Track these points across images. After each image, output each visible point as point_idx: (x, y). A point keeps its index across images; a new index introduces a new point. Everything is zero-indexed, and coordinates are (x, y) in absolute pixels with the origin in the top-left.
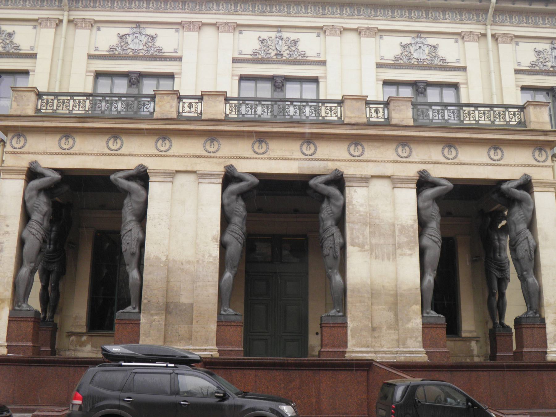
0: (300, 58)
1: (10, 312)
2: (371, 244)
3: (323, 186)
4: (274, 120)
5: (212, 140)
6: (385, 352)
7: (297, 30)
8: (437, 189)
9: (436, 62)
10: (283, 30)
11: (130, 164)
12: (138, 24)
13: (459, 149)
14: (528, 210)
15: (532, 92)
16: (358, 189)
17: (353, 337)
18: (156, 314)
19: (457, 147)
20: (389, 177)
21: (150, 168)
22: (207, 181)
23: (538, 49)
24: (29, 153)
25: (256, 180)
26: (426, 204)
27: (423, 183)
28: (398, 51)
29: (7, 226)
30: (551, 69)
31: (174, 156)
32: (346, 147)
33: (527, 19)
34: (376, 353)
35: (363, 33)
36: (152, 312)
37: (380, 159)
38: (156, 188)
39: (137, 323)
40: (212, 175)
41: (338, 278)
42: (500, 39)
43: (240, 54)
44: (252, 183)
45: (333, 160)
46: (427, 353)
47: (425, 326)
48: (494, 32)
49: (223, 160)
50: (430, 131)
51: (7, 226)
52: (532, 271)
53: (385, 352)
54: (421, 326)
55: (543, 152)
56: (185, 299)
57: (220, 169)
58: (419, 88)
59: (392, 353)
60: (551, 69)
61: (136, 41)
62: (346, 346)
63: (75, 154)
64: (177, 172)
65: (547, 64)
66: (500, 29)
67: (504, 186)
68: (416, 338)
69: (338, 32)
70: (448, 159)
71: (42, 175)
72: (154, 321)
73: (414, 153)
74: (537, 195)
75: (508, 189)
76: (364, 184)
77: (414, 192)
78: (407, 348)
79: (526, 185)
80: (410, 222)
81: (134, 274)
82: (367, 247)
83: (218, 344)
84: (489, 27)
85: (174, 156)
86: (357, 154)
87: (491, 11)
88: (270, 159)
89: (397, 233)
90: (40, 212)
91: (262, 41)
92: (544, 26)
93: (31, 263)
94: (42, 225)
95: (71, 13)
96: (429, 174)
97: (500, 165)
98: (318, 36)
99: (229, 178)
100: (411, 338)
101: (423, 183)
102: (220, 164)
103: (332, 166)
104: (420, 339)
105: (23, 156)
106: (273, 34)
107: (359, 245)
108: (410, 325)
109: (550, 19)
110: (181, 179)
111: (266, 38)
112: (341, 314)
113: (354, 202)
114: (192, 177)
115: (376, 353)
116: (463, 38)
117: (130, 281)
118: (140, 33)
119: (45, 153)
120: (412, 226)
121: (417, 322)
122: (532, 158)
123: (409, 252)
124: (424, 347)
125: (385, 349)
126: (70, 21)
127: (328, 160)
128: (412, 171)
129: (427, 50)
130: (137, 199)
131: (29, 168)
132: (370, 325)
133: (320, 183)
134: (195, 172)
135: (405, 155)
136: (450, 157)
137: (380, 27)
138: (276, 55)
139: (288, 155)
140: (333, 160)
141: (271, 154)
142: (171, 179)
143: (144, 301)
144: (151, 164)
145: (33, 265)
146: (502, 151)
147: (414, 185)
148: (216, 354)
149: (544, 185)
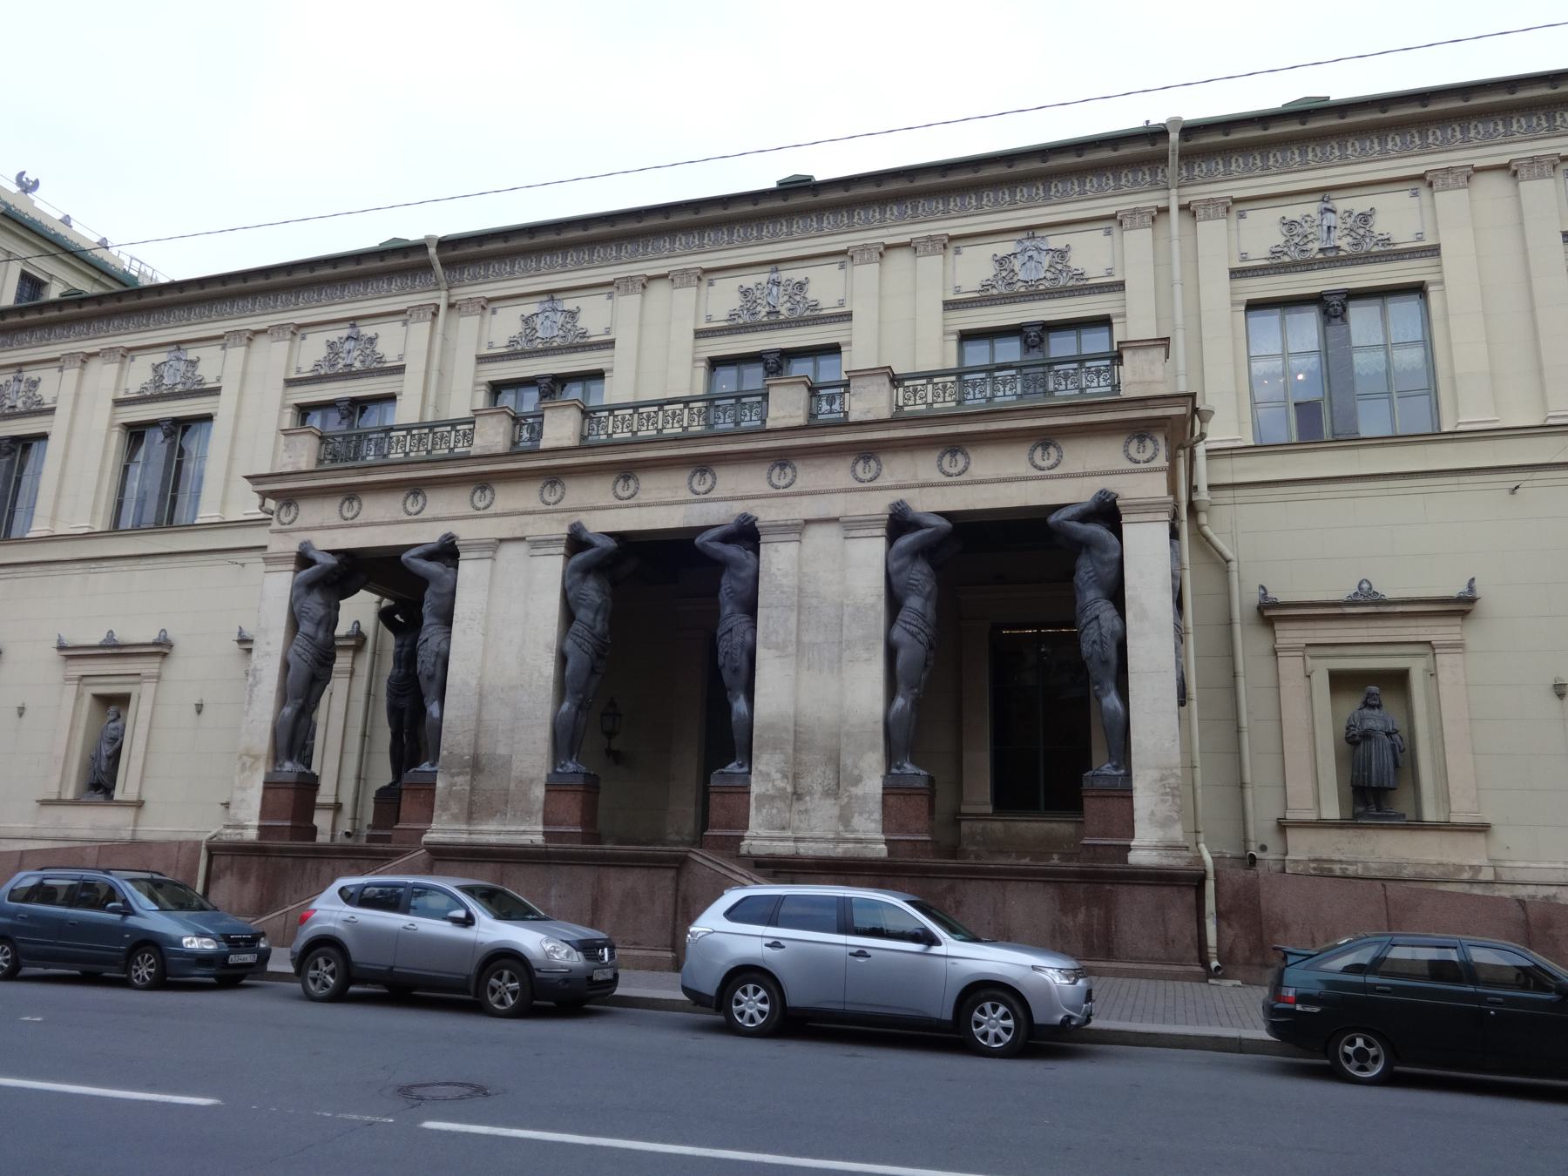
0: (808, 313)
1: (267, 774)
2: (799, 643)
3: (717, 546)
4: (710, 432)
5: (626, 478)
6: (814, 840)
7: (806, 263)
8: (919, 533)
9: (1063, 281)
10: (780, 267)
11: (430, 535)
12: (551, 293)
13: (972, 455)
14: (1103, 563)
15: (1379, 301)
16: (781, 546)
17: (758, 809)
18: (459, 774)
19: (968, 450)
20: (836, 520)
22: (542, 551)
23: (1289, 218)
24: (299, 530)
25: (611, 544)
26: (900, 562)
27: (899, 523)
28: (988, 271)
30: (1320, 256)
31: (496, 515)
32: (765, 473)
33: (1265, 158)
34: (796, 840)
35: (921, 248)
37: (829, 488)
38: (468, 569)
39: (431, 788)
40: (549, 542)
41: (740, 706)
42: (1200, 213)
43: (709, 321)
44: (604, 550)
45: (742, 498)
46: (887, 842)
47: (888, 791)
48: (1185, 201)
49: (564, 515)
50: (908, 427)
52: (1111, 685)
53: (814, 840)
54: (880, 791)
55: (1148, 443)
56: (502, 750)
57: (563, 531)
58: (1028, 337)
59: (827, 840)
60: (1320, 256)
61: (548, 323)
62: (747, 828)
63: (361, 525)
64: (501, 540)
65: (1310, 246)
66: (1197, 193)
67: (1053, 519)
68: (871, 813)
69: (876, 255)
70: (777, 488)
71: (311, 562)
73: (885, 470)
74: (1128, 531)
75: (1058, 523)
76: (793, 536)
77: (880, 545)
78: (854, 831)
79: (1107, 513)
80: (871, 600)
81: (433, 709)
82: (792, 649)
83: (546, 823)
84: (1174, 192)
85: (496, 515)
86: (783, 483)
87: (1173, 159)
88: (639, 506)
89: (846, 618)
90: (311, 619)
91: (745, 293)
92: (1305, 167)
95: (453, 291)
96: (908, 507)
97: (1052, 477)
98: (842, 267)
99: (576, 542)
100: (861, 814)
101: (899, 523)
102: (562, 521)
103: (739, 508)
104: (878, 815)
106: (763, 277)
107: (777, 647)
108: (858, 791)
109: (1318, 150)
110: (509, 552)
111: (752, 286)
112: (745, 769)
113: (773, 570)
114: (521, 548)
115: (796, 840)
116: (1121, 223)
117: (428, 720)
118: (554, 310)
120: (873, 606)
121: (873, 784)
122: (1121, 455)
123: (865, 656)
124: (883, 832)
125: (817, 833)
126: (451, 306)
127: (733, 499)
128: (878, 505)
129: (1046, 260)
130: (438, 590)
132: (790, 789)
133: (711, 540)
134: (522, 539)
135: (869, 476)
136: (954, 471)
137: (952, 233)
138: (769, 313)
139: (667, 496)
140: (742, 498)
141: (642, 497)
142: (490, 554)
143: (443, 753)
144: (465, 532)
146: (1059, 449)
147: (882, 531)
148: (539, 839)
149: (1146, 507)
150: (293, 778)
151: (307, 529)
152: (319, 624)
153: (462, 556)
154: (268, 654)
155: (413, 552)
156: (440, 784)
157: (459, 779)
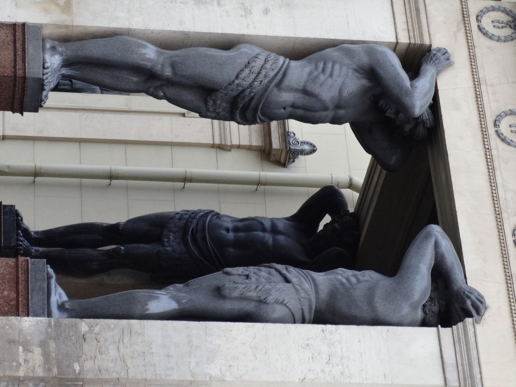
1: (38, 28)
18: (46, 355)
21: (478, 327)
24: (471, 47)
29: (266, 11)
36: (52, 345)
39: (19, 307)
51: (266, 11)
72: (27, 350)
81: (163, 301)
90: (312, 78)
93: (173, 65)
94: (279, 85)
105: (462, 36)
117: (141, 293)
119: (477, 84)
130: (379, 294)
131: (429, 49)
143: (84, 325)
145: (168, 72)
150: (33, 70)
151: (472, 59)
152: (305, 92)
153: (446, 332)
154: (248, 12)
155: (446, 245)
156: (28, 323)
157: (36, 356)
